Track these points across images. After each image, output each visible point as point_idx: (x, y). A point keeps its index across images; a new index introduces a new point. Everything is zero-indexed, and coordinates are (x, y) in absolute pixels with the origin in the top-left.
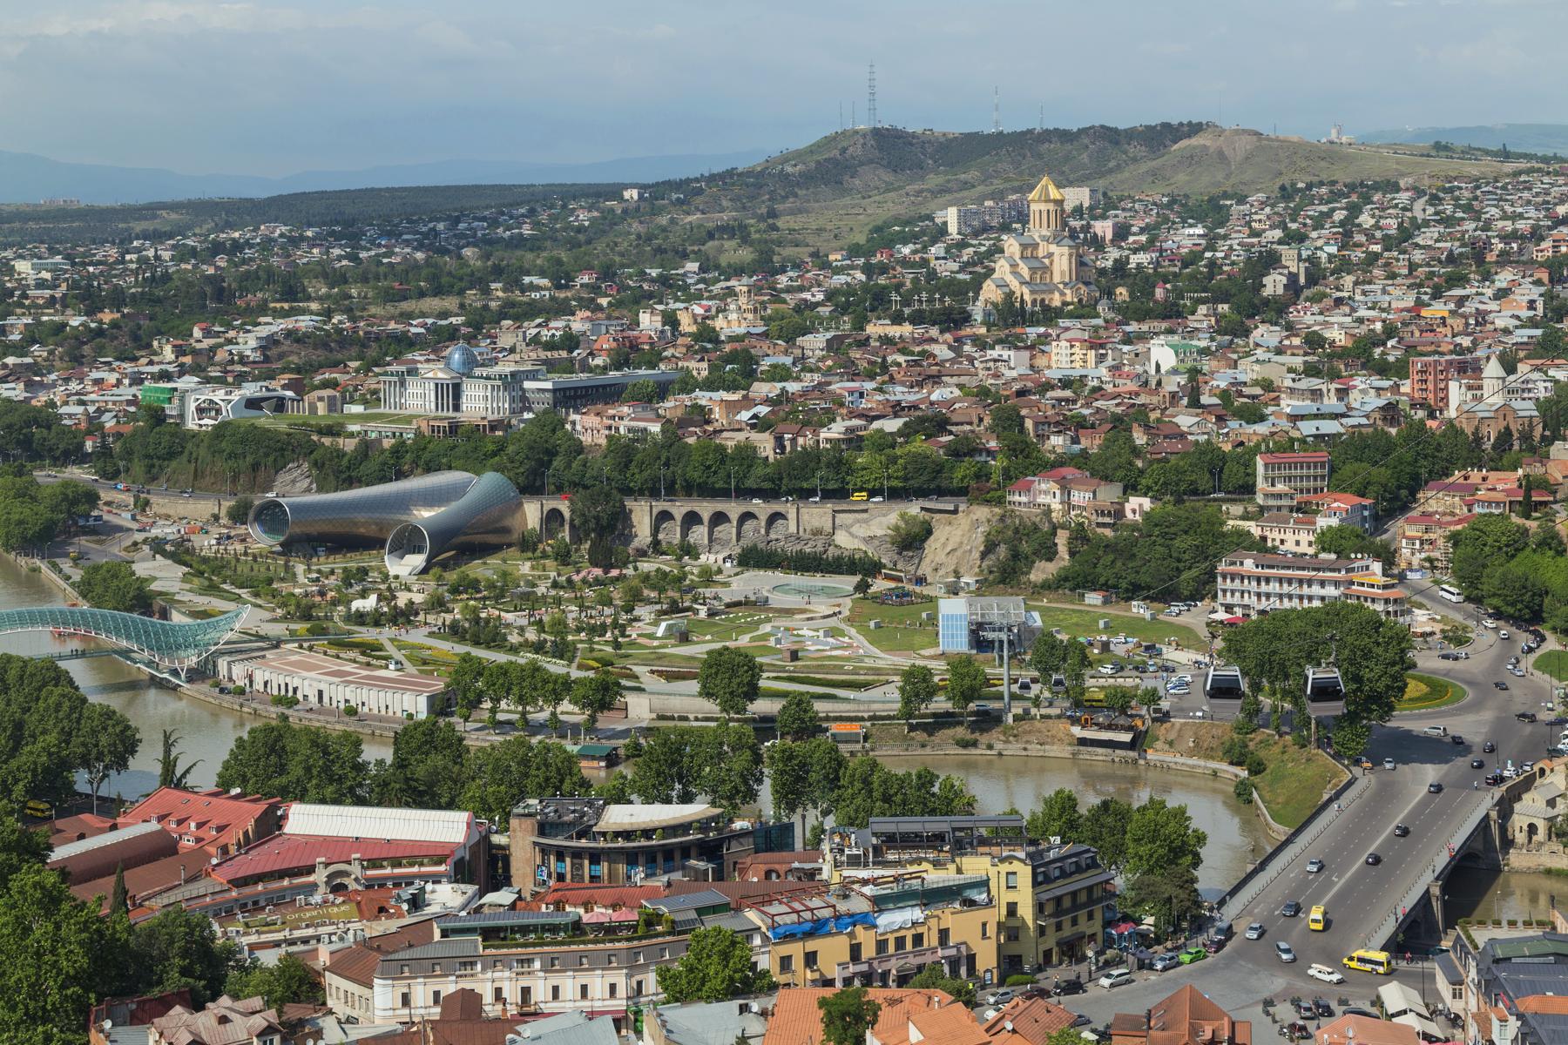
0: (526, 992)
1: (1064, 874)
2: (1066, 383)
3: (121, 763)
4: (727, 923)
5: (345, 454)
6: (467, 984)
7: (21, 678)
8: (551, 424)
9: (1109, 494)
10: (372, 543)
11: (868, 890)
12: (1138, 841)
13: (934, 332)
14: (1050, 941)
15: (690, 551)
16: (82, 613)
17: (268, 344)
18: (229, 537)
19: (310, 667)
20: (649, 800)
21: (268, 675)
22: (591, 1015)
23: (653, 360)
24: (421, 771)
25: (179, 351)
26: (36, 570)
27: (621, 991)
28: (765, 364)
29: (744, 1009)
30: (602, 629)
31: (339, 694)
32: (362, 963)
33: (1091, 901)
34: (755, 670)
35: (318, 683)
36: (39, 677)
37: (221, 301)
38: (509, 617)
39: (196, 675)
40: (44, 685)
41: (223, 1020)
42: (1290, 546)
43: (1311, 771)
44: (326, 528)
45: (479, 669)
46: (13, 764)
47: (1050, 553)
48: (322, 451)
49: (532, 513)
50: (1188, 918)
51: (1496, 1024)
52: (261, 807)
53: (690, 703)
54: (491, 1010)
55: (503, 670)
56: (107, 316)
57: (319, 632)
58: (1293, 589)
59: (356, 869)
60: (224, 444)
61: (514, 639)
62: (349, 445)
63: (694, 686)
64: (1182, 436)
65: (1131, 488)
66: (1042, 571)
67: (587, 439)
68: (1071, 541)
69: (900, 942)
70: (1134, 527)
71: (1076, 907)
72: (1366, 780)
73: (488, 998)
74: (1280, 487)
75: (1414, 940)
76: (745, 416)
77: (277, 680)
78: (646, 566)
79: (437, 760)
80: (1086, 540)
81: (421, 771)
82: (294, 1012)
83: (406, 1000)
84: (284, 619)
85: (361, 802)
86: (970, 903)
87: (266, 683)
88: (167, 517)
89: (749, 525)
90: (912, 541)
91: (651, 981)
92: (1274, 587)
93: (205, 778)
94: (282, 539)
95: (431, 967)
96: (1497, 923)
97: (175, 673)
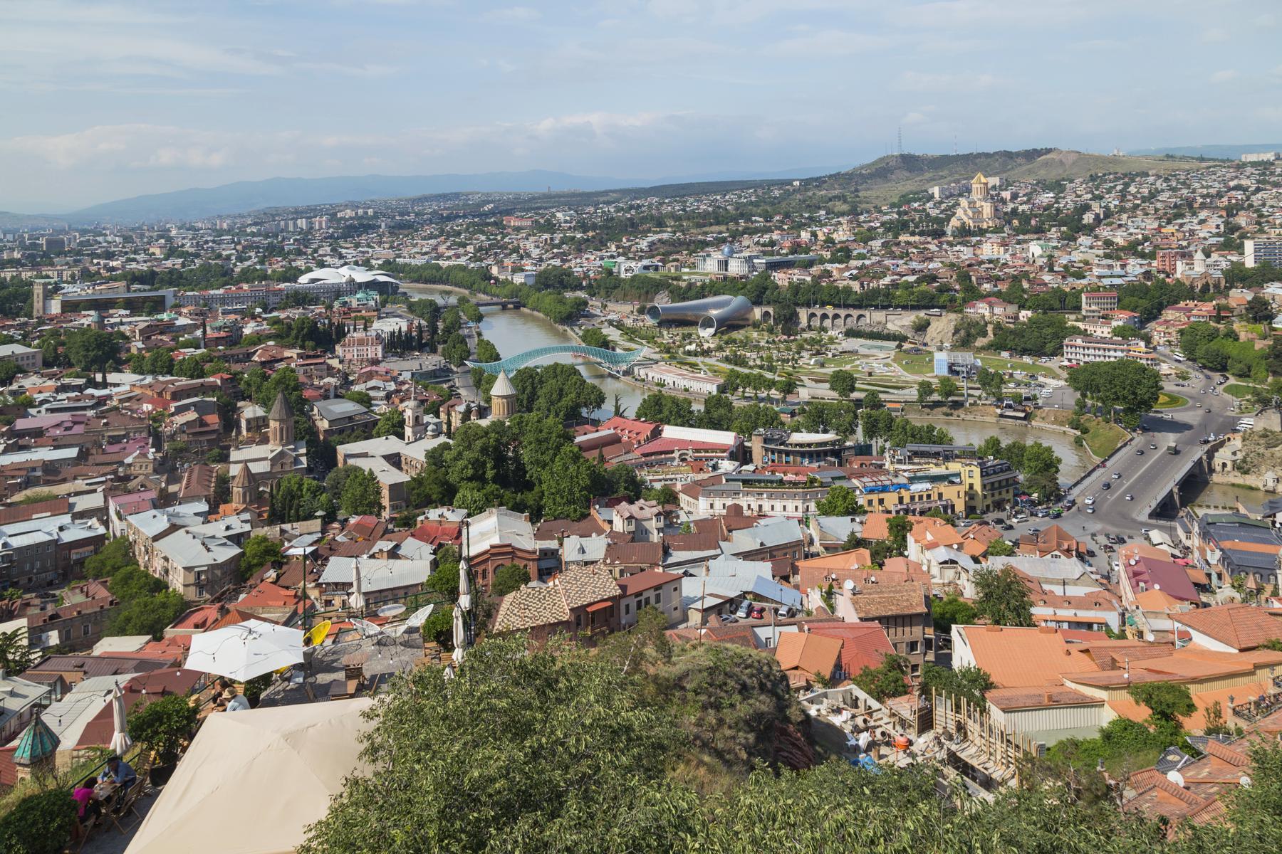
0: (760, 506)
1: (995, 473)
2: (990, 261)
3: (599, 407)
4: (845, 484)
6: (736, 502)
8: (765, 277)
9: (1012, 309)
10: (693, 323)
11: (906, 474)
12: (1029, 460)
13: (929, 239)
14: (989, 501)
15: (824, 330)
17: (652, 244)
19: (670, 372)
20: (809, 431)
21: (654, 374)
22: (788, 518)
23: (807, 251)
24: (715, 415)
25: (618, 247)
27: (800, 509)
28: (855, 253)
29: (853, 520)
30: (788, 361)
31: (682, 383)
32: (695, 490)
33: (1008, 485)
34: (853, 380)
35: (673, 378)
37: (634, 227)
38: (748, 355)
39: (626, 373)
41: (641, 509)
42: (1099, 333)
43: (1111, 434)
45: (738, 375)
47: (985, 334)
49: (757, 313)
50: (1054, 495)
51: (1209, 553)
52: (653, 426)
53: (826, 393)
54: (746, 513)
55: (748, 376)
56: (591, 234)
57: (673, 358)
58: (1101, 353)
59: (690, 453)
61: (751, 363)
62: (683, 284)
63: (827, 385)
64: (1046, 284)
65: (1022, 307)
66: (981, 342)
67: (780, 283)
68: (994, 329)
69: (921, 497)
70: (1024, 324)
71: (1000, 487)
72: (1139, 439)
73: (745, 508)
74: (1094, 307)
75: (1165, 511)
76: (847, 274)
77: (657, 376)
78: (805, 335)
79: (722, 411)
80: (1001, 329)
81: (715, 415)
82: (668, 507)
83: (712, 506)
85: (691, 426)
86: (953, 483)
89: (849, 319)
90: (922, 327)
91: (813, 506)
92: (1091, 351)
93: (631, 413)
95: (722, 493)
96: (1208, 507)
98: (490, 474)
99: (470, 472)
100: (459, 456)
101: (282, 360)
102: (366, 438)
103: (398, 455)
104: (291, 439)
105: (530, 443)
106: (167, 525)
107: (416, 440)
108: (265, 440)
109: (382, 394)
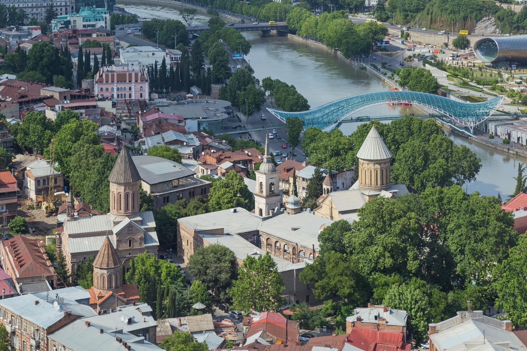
5: (515, 14)
7: (420, 129)
16: (401, 93)
18: (458, 56)
26: (364, 68)
36: (429, 129)
40: (432, 133)
44: (516, 54)
46: (426, 173)
48: (502, 11)
60: (447, 6)
84: (513, 103)
87: (518, 139)
88: (420, 43)
94: (493, 59)
97: (466, 128)
98: (412, 265)
99: (388, 262)
100: (370, 241)
101: (41, 100)
102: (207, 211)
103: (256, 233)
104: (137, 209)
105: (459, 227)
106: (62, 315)
107: (274, 215)
108: (104, 209)
109: (189, 151)
